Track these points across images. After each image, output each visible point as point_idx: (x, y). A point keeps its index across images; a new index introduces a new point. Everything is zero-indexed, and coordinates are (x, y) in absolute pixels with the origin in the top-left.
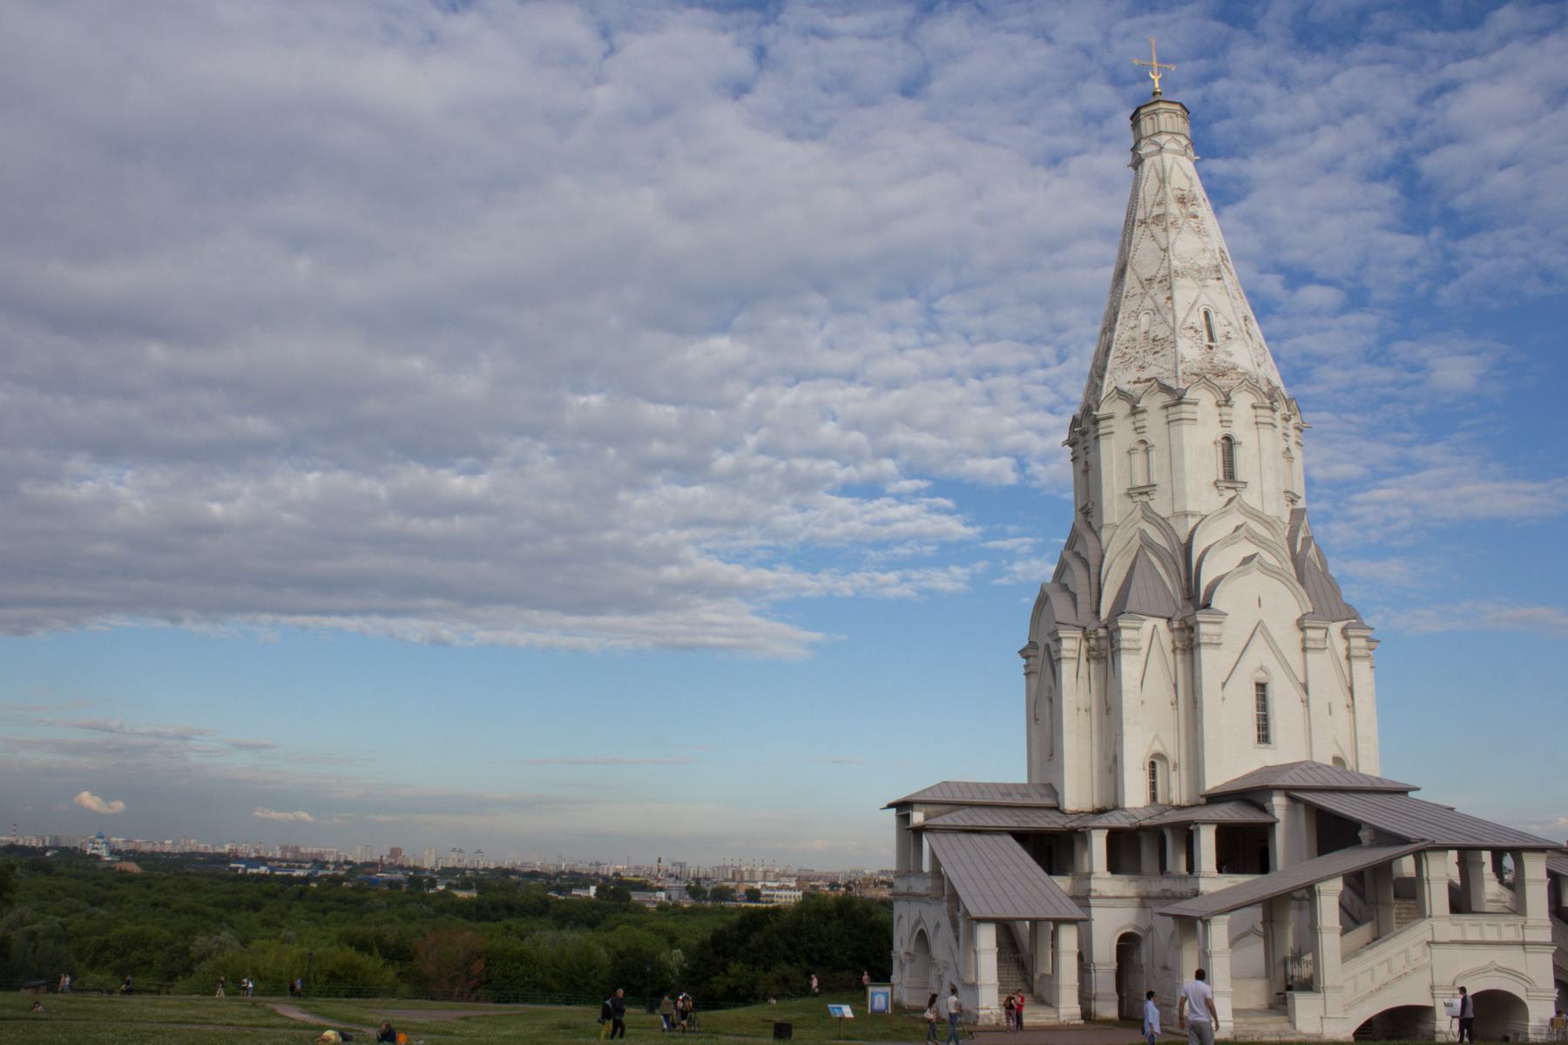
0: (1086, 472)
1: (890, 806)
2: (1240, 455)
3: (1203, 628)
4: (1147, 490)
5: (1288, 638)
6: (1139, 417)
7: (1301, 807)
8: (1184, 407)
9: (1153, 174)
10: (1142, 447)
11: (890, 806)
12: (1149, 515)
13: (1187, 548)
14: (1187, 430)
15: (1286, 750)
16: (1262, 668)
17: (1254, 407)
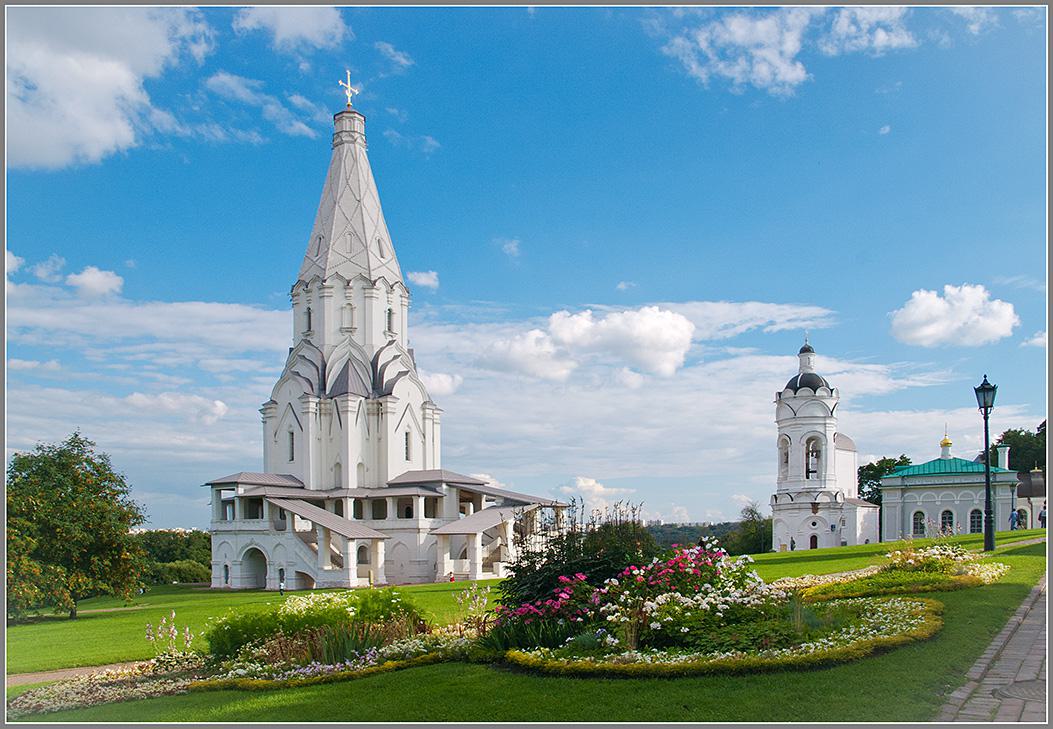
0: (309, 312)
1: (207, 484)
2: (396, 319)
3: (389, 404)
4: (351, 330)
5: (419, 414)
6: (348, 291)
7: (455, 490)
8: (374, 291)
9: (349, 154)
10: (348, 307)
11: (207, 484)
12: (352, 344)
13: (374, 364)
14: (374, 301)
15: (415, 465)
16: (408, 426)
17: (401, 296)
